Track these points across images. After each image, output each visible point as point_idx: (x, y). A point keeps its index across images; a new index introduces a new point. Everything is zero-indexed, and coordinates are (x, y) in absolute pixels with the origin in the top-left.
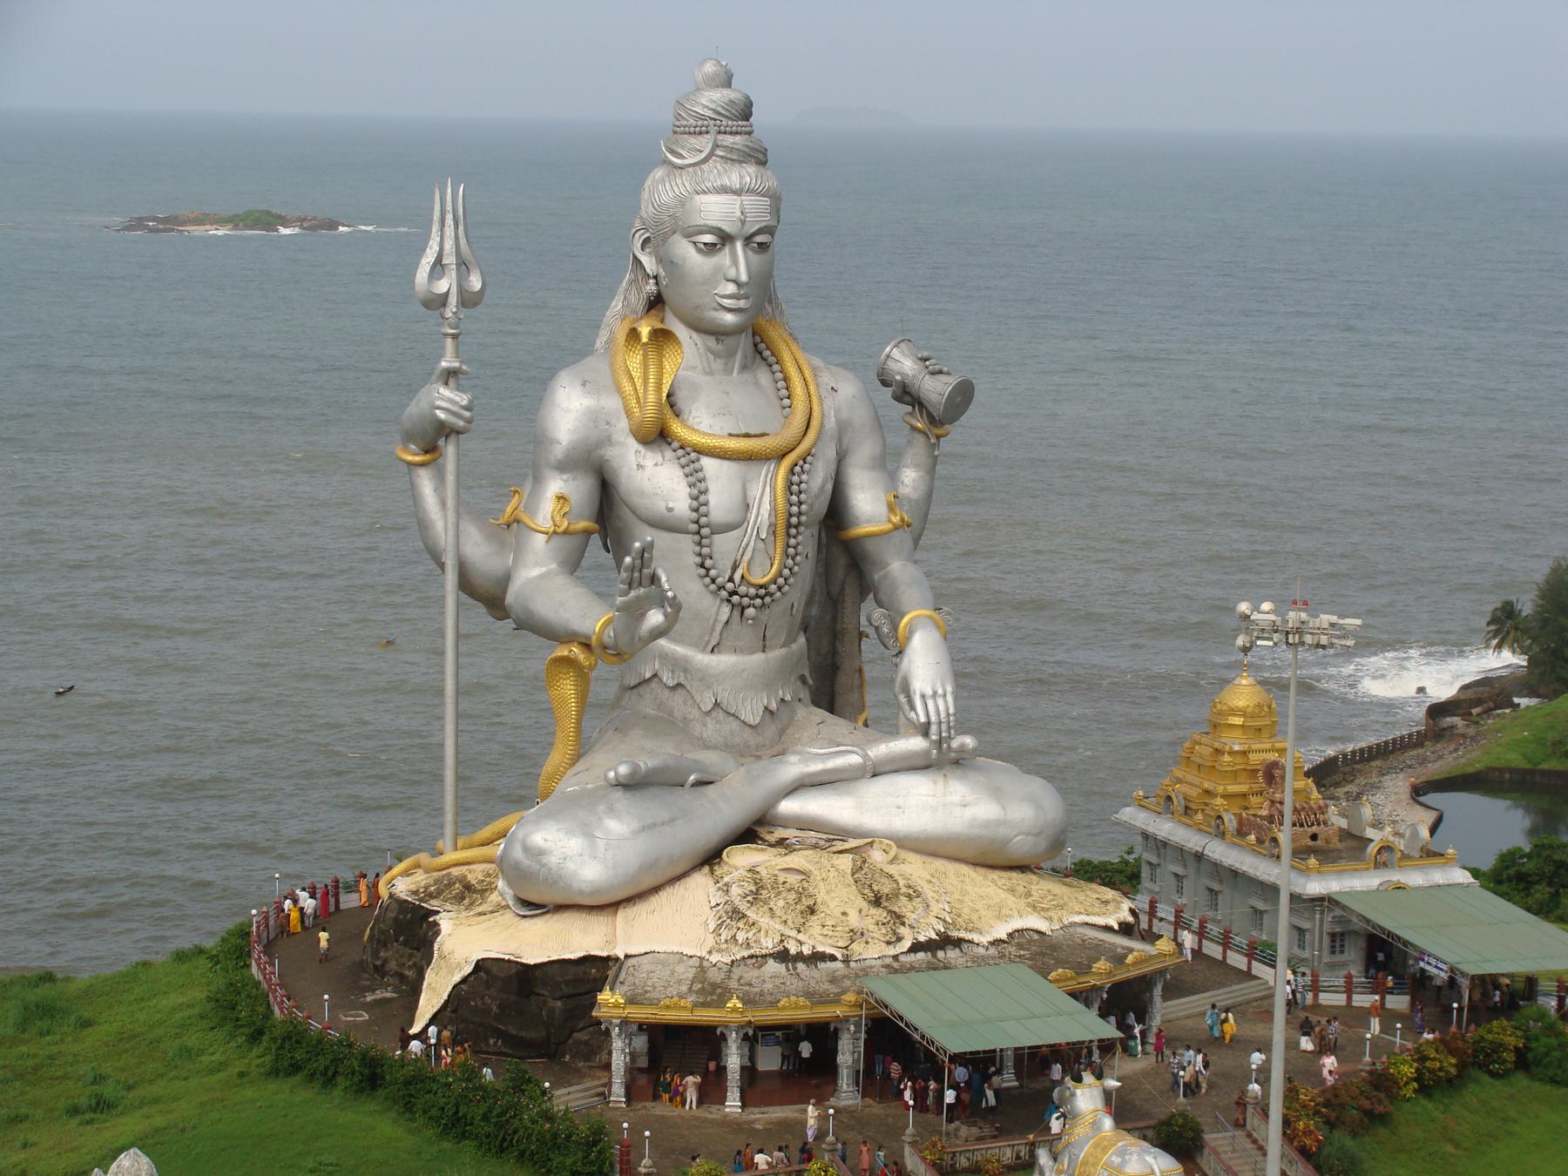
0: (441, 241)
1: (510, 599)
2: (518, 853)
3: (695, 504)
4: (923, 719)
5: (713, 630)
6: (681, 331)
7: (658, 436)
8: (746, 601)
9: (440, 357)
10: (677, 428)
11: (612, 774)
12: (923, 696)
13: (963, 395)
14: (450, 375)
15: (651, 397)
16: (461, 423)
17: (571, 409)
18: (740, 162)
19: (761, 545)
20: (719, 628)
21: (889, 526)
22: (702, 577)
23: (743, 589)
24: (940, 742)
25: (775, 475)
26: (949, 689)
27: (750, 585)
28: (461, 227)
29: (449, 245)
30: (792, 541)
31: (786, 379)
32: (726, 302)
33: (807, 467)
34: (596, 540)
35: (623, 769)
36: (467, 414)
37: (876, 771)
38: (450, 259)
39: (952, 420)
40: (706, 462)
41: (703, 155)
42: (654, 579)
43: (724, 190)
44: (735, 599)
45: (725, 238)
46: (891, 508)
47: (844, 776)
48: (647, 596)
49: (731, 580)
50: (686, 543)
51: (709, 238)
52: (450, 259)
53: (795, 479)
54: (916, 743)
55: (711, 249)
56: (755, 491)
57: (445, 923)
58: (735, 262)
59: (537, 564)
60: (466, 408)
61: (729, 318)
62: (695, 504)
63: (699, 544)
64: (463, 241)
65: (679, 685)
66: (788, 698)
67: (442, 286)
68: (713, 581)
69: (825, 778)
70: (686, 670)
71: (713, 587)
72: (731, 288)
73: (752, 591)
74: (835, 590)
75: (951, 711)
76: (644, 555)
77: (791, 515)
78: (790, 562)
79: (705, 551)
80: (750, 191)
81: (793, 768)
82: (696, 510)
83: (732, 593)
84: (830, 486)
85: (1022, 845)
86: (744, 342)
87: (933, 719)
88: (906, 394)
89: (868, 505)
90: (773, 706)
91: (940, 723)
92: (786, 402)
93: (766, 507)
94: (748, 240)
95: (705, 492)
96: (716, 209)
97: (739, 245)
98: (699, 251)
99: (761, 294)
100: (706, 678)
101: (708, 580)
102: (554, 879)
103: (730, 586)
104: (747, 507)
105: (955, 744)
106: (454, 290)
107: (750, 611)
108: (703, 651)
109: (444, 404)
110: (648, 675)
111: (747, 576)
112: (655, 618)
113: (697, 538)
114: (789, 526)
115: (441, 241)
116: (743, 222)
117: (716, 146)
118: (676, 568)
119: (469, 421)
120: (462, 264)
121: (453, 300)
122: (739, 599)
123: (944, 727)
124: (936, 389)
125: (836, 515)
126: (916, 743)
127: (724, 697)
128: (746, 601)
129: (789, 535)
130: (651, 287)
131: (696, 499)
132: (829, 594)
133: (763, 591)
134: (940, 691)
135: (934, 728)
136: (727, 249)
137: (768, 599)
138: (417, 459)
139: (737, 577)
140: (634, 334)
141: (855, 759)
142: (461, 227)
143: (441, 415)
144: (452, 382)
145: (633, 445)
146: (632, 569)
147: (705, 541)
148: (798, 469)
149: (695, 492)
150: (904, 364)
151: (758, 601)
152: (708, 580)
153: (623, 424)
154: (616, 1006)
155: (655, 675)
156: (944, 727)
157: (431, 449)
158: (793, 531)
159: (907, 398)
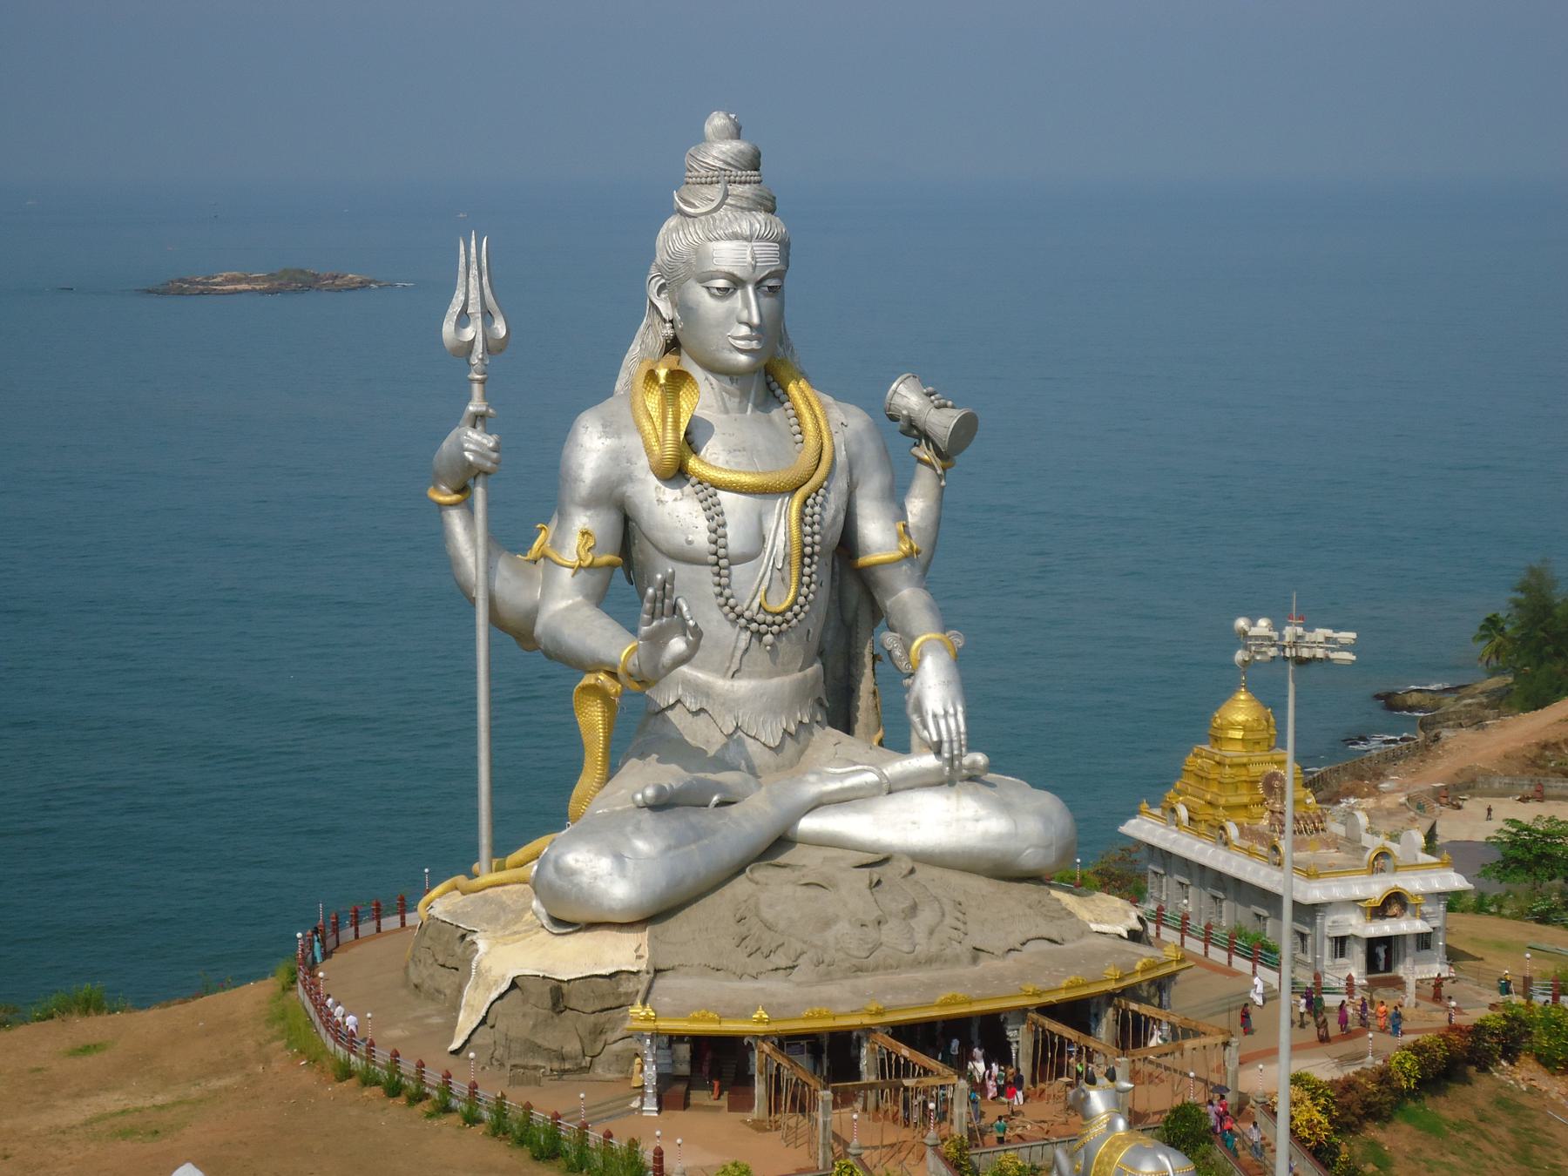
0: (470, 290)
1: (539, 629)
2: (550, 872)
3: (714, 536)
4: (935, 738)
5: (733, 656)
6: (697, 373)
7: (676, 474)
9: (469, 398)
10: (693, 463)
11: (639, 797)
12: (935, 716)
13: (966, 429)
14: (478, 419)
15: (670, 436)
16: (489, 464)
17: (592, 449)
18: (750, 210)
19: (777, 574)
20: (738, 654)
23: (761, 617)
24: (952, 759)
25: (789, 508)
26: (960, 709)
27: (767, 612)
28: (485, 279)
29: (474, 295)
30: (807, 570)
32: (741, 344)
34: (620, 573)
35: (650, 792)
36: (495, 455)
37: (892, 788)
38: (474, 308)
39: (958, 451)
40: (723, 496)
41: (714, 204)
42: (675, 609)
43: (735, 237)
44: (754, 626)
45: (736, 283)
46: (900, 538)
47: (861, 794)
48: (669, 625)
50: (706, 573)
51: (721, 283)
52: (474, 308)
53: (808, 510)
54: (929, 761)
55: (725, 293)
56: (770, 524)
57: (482, 945)
58: (747, 305)
59: (564, 597)
60: (494, 450)
61: (743, 359)
62: (714, 536)
64: (487, 291)
65: (702, 710)
66: (806, 720)
67: (469, 333)
68: (732, 608)
69: (842, 797)
70: (708, 695)
71: (732, 616)
72: (744, 330)
73: (769, 619)
74: (849, 616)
75: (962, 729)
76: (666, 586)
78: (804, 590)
79: (724, 581)
80: (760, 238)
81: (813, 787)
82: (715, 542)
83: (752, 620)
84: (842, 517)
85: (1031, 858)
86: (757, 384)
87: (945, 737)
88: (914, 430)
89: (877, 536)
90: (792, 728)
91: (951, 741)
92: (799, 437)
93: (781, 538)
94: (758, 284)
95: (724, 525)
96: (729, 255)
97: (750, 289)
98: (713, 295)
99: (771, 333)
100: (730, 704)
101: (727, 609)
102: (585, 898)
103: (747, 614)
104: (763, 540)
105: (966, 761)
106: (480, 337)
107: (769, 638)
108: (724, 676)
109: (472, 447)
110: (672, 701)
112: (677, 645)
114: (803, 555)
115: (470, 290)
116: (754, 267)
117: (726, 195)
118: (696, 596)
119: (496, 462)
120: (487, 315)
121: (479, 347)
122: (760, 629)
123: (956, 745)
124: (942, 422)
125: (847, 544)
126: (929, 761)
127: (744, 720)
128: (764, 627)
129: (803, 565)
130: (668, 331)
131: (715, 531)
132: (843, 620)
133: (779, 619)
134: (951, 711)
135: (946, 746)
136: (739, 293)
137: (785, 626)
138: (448, 499)
139: (755, 605)
140: (652, 376)
141: (871, 777)
142: (485, 279)
143: (469, 456)
145: (653, 481)
146: (654, 600)
147: (724, 572)
148: (810, 501)
149: (714, 525)
150: (908, 397)
151: (775, 628)
152: (727, 609)
153: (643, 462)
154: (647, 1019)
155: (678, 701)
156: (956, 745)
157: (463, 489)
158: (807, 560)
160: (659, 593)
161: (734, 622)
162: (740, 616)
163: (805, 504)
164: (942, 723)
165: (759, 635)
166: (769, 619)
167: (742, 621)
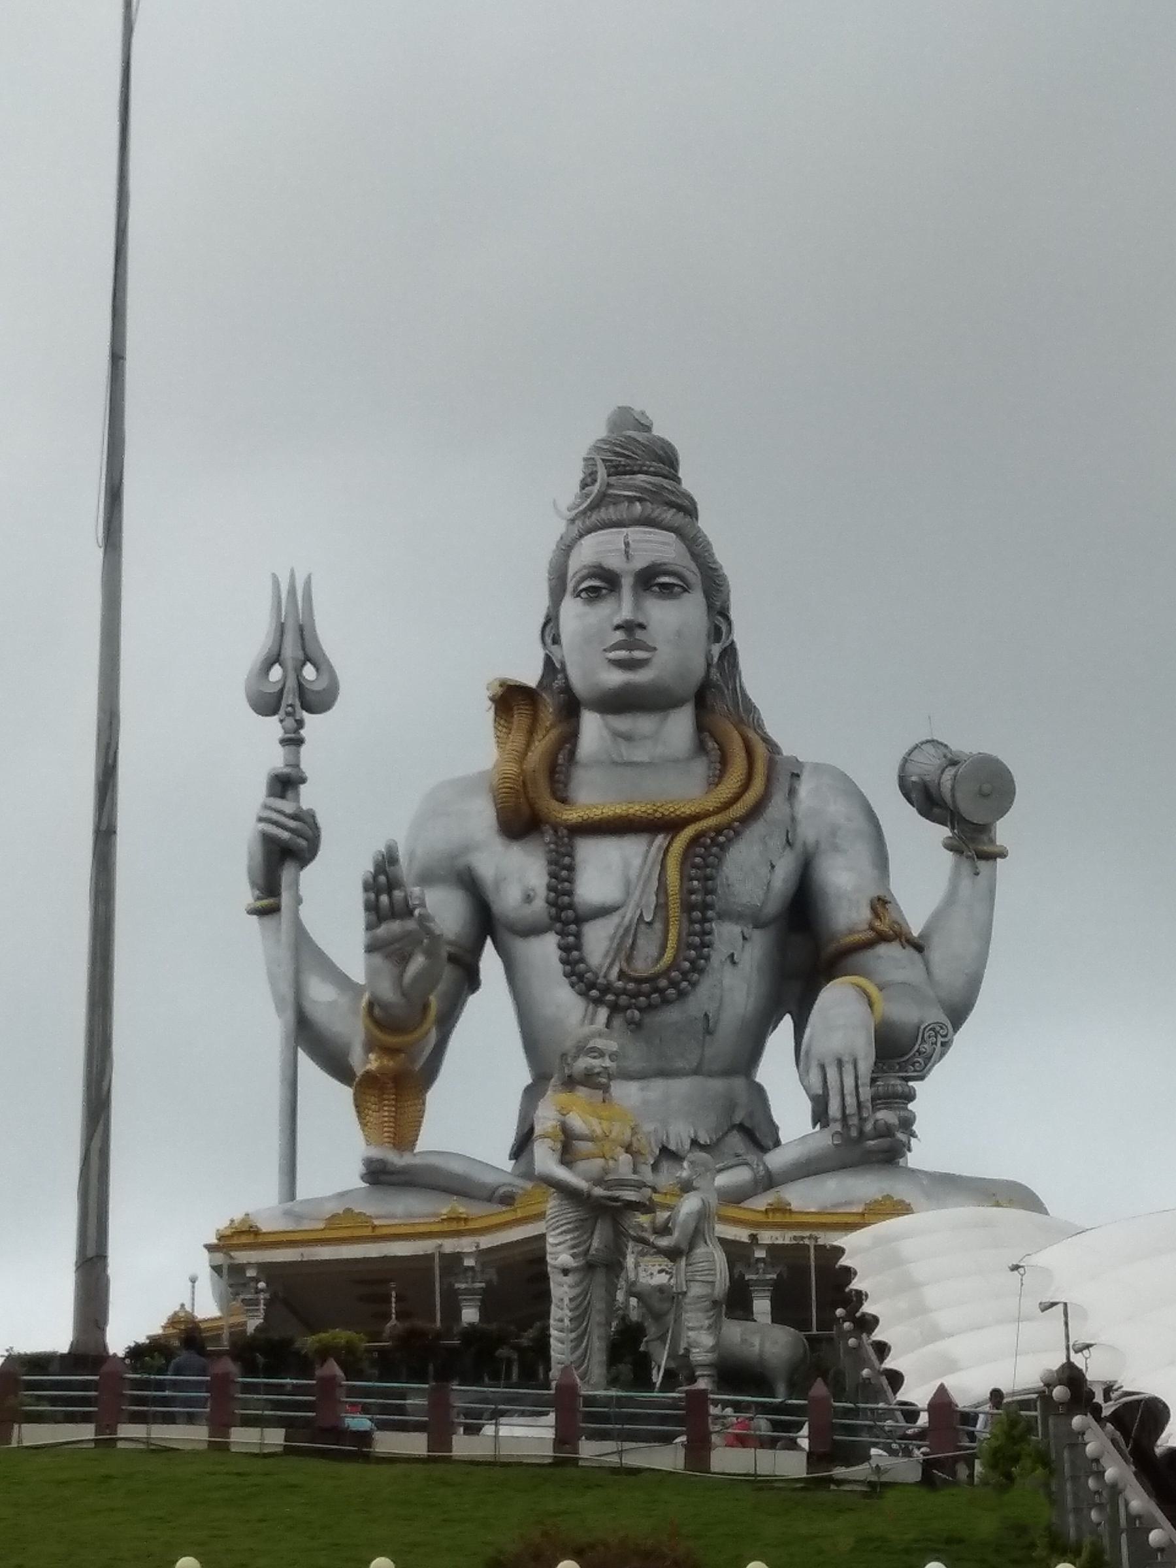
8: (623, 1000)
12: (823, 1068)
19: (643, 927)
21: (871, 935)
22: (567, 975)
23: (620, 984)
31: (724, 761)
32: (613, 655)
33: (721, 839)
49: (605, 977)
55: (593, 595)
63: (562, 934)
72: (619, 636)
77: (692, 892)
97: (627, 583)
101: (574, 978)
111: (625, 968)
113: (558, 926)
114: (688, 908)
128: (623, 1000)
133: (646, 987)
144: (290, 794)
159: (936, 810)
160: (382, 879)
161: (583, 994)
162: (592, 985)
163: (695, 841)
164: (832, 1074)
165: (615, 1009)
166: (631, 986)
167: (594, 993)
